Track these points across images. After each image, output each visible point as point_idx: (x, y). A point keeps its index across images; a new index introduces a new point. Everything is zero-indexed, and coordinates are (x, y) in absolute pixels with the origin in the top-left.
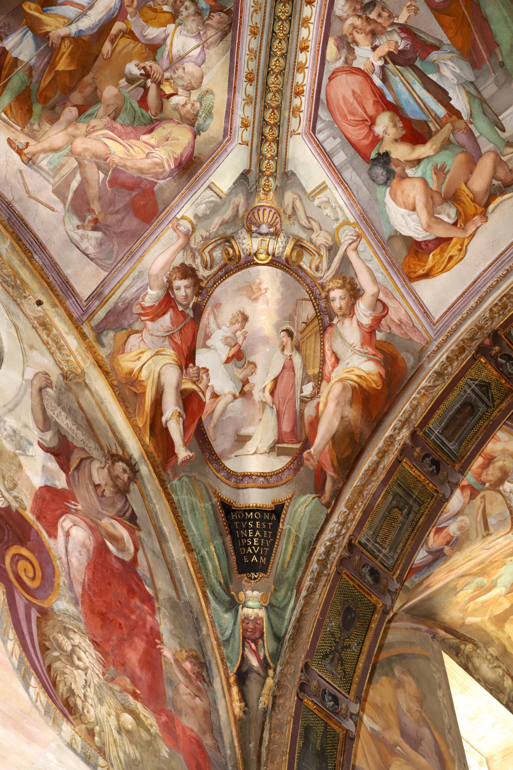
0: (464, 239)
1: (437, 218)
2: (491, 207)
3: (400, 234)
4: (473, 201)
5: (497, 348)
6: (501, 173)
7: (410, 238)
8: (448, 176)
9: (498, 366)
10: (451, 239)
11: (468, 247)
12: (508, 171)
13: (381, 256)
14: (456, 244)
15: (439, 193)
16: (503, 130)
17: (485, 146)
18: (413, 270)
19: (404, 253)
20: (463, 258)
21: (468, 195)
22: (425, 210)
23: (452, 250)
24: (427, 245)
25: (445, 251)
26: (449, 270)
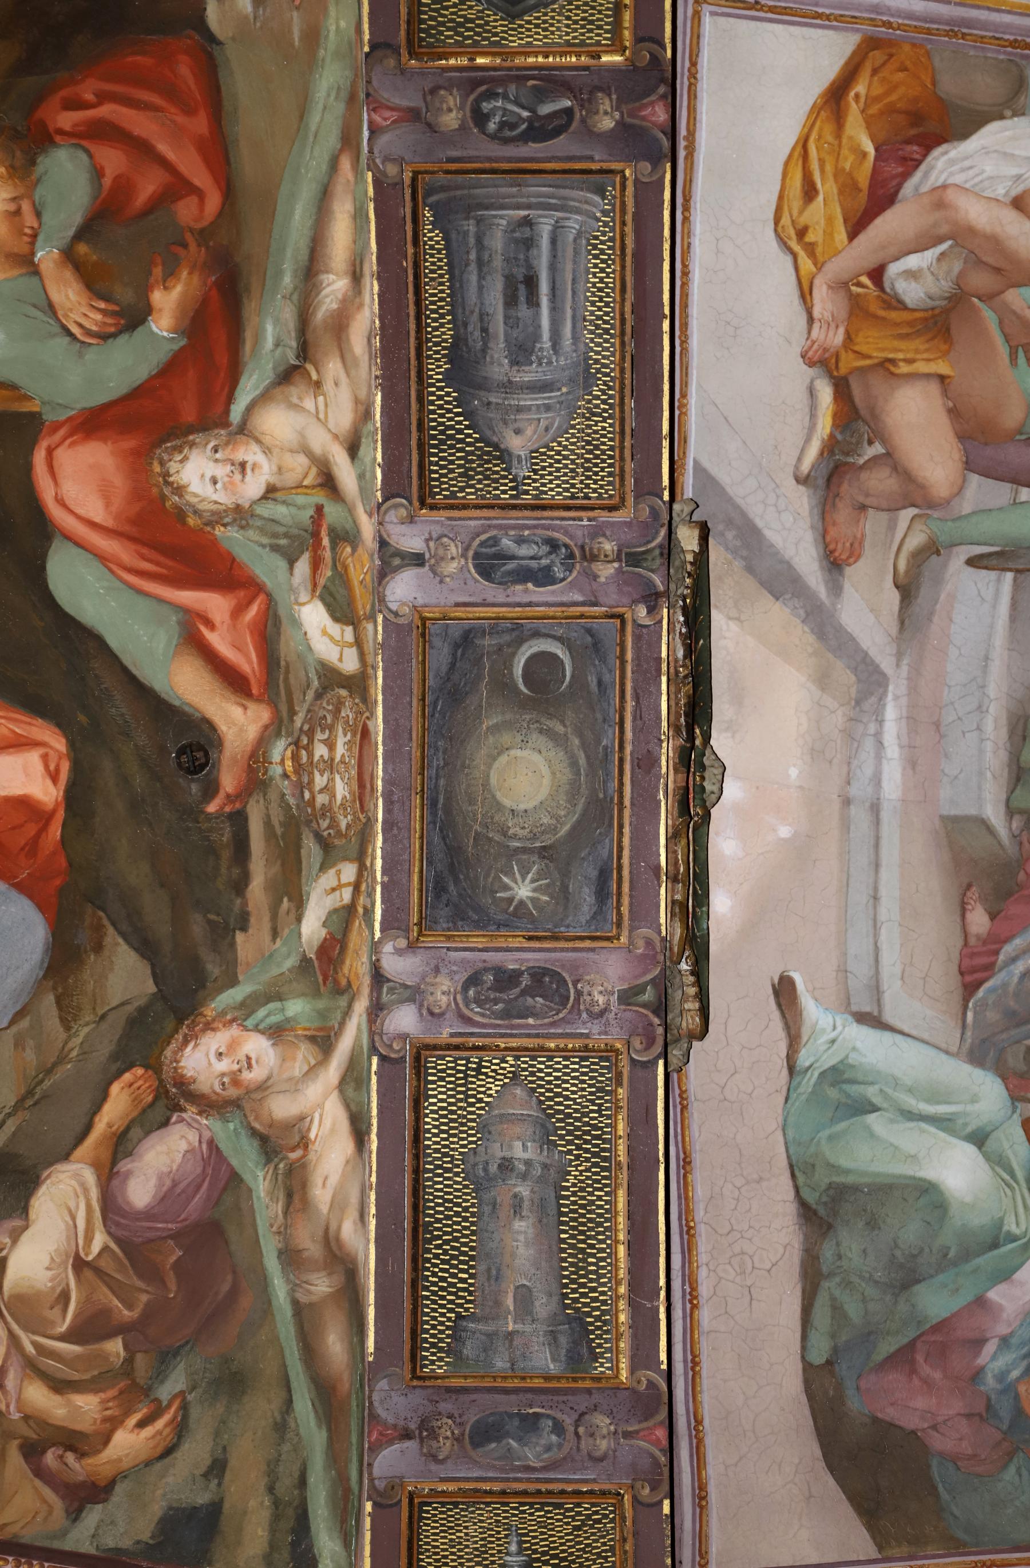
0: (819, 266)
1: (940, 240)
2: (826, 394)
3: (1002, 117)
4: (886, 365)
5: (607, 124)
6: (880, 482)
7: (964, 135)
8: (1003, 350)
9: (551, 82)
10: (852, 235)
11: (789, 259)
12: (868, 501)
13: (1007, 18)
14: (829, 234)
15: (988, 298)
16: (973, 562)
17: (981, 492)
18: (884, 73)
19: (949, 86)
20: (777, 222)
21: (910, 361)
22: (988, 229)
23: (825, 213)
24: (904, 159)
25: (841, 192)
26: (787, 164)
